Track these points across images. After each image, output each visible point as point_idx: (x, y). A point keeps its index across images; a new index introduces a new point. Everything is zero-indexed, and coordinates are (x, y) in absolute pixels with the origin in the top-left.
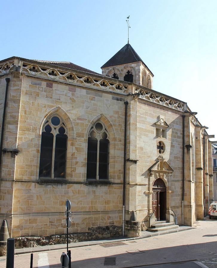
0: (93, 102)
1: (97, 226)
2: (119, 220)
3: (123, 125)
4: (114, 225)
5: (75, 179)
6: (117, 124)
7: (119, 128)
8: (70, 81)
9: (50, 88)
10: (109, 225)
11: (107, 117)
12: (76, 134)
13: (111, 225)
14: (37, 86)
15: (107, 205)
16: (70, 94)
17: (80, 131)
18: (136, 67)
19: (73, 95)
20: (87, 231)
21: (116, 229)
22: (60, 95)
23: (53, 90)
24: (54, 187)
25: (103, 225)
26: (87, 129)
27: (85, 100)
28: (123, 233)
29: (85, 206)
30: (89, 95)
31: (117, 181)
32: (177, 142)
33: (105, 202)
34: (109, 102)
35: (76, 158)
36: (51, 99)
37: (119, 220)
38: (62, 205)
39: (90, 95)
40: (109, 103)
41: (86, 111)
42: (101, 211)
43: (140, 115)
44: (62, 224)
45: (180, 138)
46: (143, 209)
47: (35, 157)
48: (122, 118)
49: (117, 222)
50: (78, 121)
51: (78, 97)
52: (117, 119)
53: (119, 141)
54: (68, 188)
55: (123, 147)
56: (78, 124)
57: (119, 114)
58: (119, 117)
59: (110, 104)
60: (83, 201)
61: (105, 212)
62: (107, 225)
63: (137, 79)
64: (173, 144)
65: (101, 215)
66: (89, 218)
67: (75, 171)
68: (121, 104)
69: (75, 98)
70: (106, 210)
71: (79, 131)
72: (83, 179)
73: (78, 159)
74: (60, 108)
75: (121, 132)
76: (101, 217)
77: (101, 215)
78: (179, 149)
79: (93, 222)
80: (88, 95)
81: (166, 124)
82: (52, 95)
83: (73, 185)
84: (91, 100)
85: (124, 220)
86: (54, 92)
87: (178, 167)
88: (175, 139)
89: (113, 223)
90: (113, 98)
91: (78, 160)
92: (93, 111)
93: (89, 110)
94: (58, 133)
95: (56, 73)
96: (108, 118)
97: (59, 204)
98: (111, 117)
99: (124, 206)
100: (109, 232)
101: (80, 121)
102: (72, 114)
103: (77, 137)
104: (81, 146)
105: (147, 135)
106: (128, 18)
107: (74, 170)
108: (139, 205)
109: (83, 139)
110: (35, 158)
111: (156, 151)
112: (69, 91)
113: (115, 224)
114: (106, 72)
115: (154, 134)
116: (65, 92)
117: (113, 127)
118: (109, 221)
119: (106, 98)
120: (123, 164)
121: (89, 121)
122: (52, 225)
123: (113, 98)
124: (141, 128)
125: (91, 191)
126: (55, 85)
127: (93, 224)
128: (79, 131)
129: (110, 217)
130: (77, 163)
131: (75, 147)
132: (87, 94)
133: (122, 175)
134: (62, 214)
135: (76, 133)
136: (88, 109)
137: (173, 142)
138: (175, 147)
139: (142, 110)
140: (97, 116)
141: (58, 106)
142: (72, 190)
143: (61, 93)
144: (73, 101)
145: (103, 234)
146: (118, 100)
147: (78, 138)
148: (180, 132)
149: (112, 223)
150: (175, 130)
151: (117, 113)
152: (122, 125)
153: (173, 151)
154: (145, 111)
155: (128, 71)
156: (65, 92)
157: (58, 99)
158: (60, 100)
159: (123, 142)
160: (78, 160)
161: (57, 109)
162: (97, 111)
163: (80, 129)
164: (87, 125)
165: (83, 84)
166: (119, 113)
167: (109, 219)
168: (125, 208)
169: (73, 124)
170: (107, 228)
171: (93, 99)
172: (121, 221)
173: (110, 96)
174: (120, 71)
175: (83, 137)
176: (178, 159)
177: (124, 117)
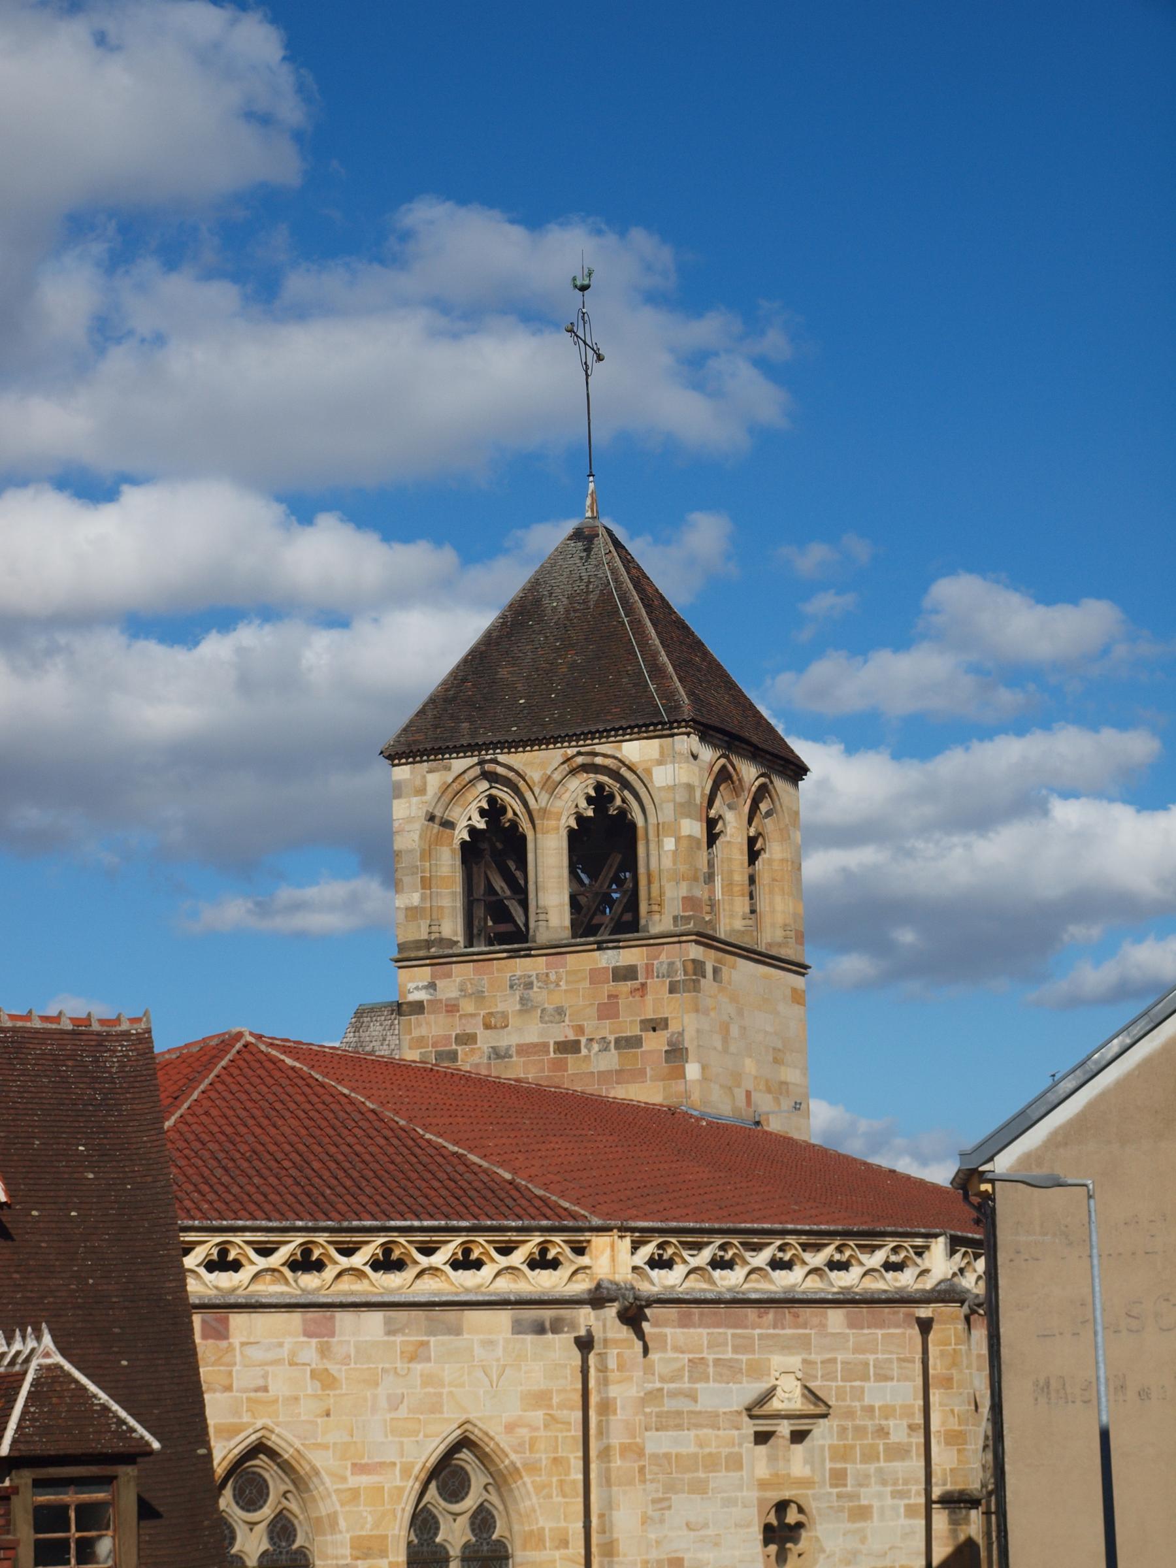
3: (572, 1461)
6: (544, 1458)
7: (554, 1480)
8: (310, 1281)
9: (218, 1342)
11: (492, 1434)
12: (351, 1548)
16: (309, 1352)
17: (368, 1526)
18: (660, 762)
19: (324, 1351)
22: (266, 1364)
23: (234, 1349)
26: (399, 1515)
27: (381, 1366)
30: (399, 1339)
32: (884, 1483)
34: (500, 1352)
36: (226, 1394)
39: (404, 1334)
40: (498, 1360)
41: (392, 1419)
43: (658, 1385)
45: (908, 1452)
48: (569, 1423)
50: (354, 1481)
52: (542, 1433)
53: (557, 1548)
56: (355, 1493)
57: (550, 1407)
58: (550, 1421)
59: (502, 1363)
63: (667, 863)
64: (864, 1502)
68: (561, 1346)
69: (333, 1368)
71: (362, 1528)
74: (272, 1432)
75: (564, 1496)
78: (903, 1521)
80: (392, 1338)
81: (812, 1398)
82: (230, 1373)
86: (238, 1358)
88: (872, 1468)
90: (518, 1328)
92: (421, 1417)
93: (403, 1412)
94: (265, 1545)
95: (240, 1258)
96: (497, 1438)
98: (510, 1428)
101: (364, 1480)
102: (325, 1447)
103: (357, 1558)
105: (699, 1488)
106: (584, 288)
112: (305, 1339)
114: (422, 791)
116: (287, 1347)
117: (527, 1479)
119: (481, 1337)
121: (406, 1472)
123: (518, 1328)
124: (667, 1456)
126: (237, 1320)
128: (362, 1528)
132: (389, 1333)
135: (351, 1538)
136: (397, 1409)
137: (863, 1490)
139: (671, 1354)
140: (445, 1435)
141: (259, 1425)
143: (270, 1356)
144: (325, 1380)
146: (540, 1329)
147: (359, 1562)
148: (905, 1423)
150: (872, 1418)
151: (541, 1399)
152: (568, 1459)
153: (863, 1540)
154: (687, 1356)
155: (599, 787)
156: (288, 1342)
157: (257, 1390)
158: (265, 1389)
161: (259, 1435)
162: (442, 1413)
163: (369, 1519)
164: (401, 1489)
165: (366, 1282)
166: (551, 1399)
169: (334, 1497)
171: (417, 1354)
173: (504, 1317)
174: (537, 790)
175: (383, 1554)
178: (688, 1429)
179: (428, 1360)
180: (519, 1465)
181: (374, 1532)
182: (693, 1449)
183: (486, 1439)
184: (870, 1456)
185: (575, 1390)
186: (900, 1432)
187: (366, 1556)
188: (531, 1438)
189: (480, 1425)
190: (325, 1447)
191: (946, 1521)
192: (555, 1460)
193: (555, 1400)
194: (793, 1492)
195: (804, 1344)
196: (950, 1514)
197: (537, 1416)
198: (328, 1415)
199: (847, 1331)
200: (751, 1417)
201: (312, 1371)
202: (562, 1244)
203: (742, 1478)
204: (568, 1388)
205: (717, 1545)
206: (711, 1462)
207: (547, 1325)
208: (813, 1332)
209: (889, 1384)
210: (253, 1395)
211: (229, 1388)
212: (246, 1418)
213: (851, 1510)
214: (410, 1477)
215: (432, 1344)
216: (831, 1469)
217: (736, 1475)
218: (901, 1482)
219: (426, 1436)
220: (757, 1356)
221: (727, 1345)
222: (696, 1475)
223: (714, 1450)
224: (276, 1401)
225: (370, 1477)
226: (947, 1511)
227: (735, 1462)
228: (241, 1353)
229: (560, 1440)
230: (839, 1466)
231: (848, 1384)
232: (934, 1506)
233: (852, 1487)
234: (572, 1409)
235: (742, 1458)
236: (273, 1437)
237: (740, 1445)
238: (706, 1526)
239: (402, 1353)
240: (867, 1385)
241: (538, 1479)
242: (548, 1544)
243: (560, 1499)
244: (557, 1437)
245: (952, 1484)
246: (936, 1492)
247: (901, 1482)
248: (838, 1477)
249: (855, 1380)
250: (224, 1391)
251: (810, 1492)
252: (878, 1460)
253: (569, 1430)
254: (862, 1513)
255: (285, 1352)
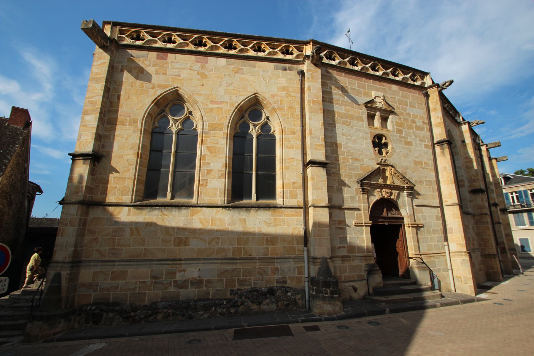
0: (239, 75)
1: (249, 287)
2: (296, 275)
3: (297, 108)
4: (286, 285)
5: (205, 199)
10: (275, 284)
11: (266, 97)
13: (279, 285)
14: (141, 59)
15: (270, 247)
16: (197, 67)
17: (216, 121)
19: (202, 67)
20: (229, 296)
21: (289, 294)
24: (164, 214)
25: (264, 287)
28: (307, 302)
29: (226, 247)
30: (232, 66)
31: (289, 202)
33: (267, 241)
35: (209, 164)
37: (296, 275)
38: (178, 246)
39: (233, 65)
42: (259, 259)
44: (175, 282)
46: (351, 255)
47: (132, 165)
48: (296, 97)
49: (292, 279)
50: (211, 106)
51: (211, 70)
53: (291, 134)
54: (192, 215)
55: (300, 143)
56: (212, 110)
57: (288, 91)
60: (220, 237)
61: (267, 259)
62: (272, 286)
65: (257, 265)
66: (233, 270)
67: (206, 185)
69: (206, 73)
70: (270, 256)
71: (213, 121)
72: (220, 199)
73: (212, 165)
76: (259, 268)
77: (257, 264)
79: (242, 278)
82: (166, 70)
83: (202, 210)
84: (236, 73)
85: (306, 275)
86: (170, 66)
87: (426, 181)
89: (285, 282)
91: (212, 166)
92: (239, 90)
93: (231, 87)
97: (172, 242)
98: (273, 96)
99: (306, 249)
100: (273, 300)
101: (215, 106)
103: (211, 130)
104: (218, 143)
107: (205, 184)
108: (340, 247)
109: (221, 133)
110: (132, 167)
111: (371, 150)
112: (196, 63)
113: (289, 284)
115: (363, 121)
116: (189, 64)
118: (276, 277)
120: (301, 171)
122: (155, 282)
125: (237, 220)
127: (241, 283)
129: (277, 269)
130: (209, 172)
131: (207, 147)
133: (300, 192)
134: (178, 262)
138: (412, 145)
140: (248, 96)
141: (175, 86)
142: (200, 219)
143: (182, 66)
145: (260, 304)
147: (211, 132)
149: (281, 280)
151: (285, 89)
159: (299, 134)
160: (212, 166)
163: (216, 118)
166: (288, 89)
167: (275, 274)
168: (308, 251)
170: (271, 291)
172: (302, 277)
175: (221, 129)
176: (424, 166)
177: (299, 95)
178: (342, 105)
179: (243, 74)
180: (276, 107)
181: (218, 122)
182: (344, 112)
183: (264, 99)
184: (410, 128)
185: (298, 87)
186: (419, 123)
187: (215, 129)
188: (281, 100)
189: (261, 94)
190: (201, 95)
191: (440, 149)
192: (290, 107)
193: (290, 90)
194: (383, 132)
195: (384, 91)
196: (440, 147)
197: (284, 94)
198: (203, 85)
199: (399, 91)
200: (366, 107)
201: (197, 72)
202: (293, 47)
203: (363, 124)
204: (295, 87)
205: (354, 142)
206: (352, 117)
207: (287, 68)
208: (387, 88)
209: (415, 109)
210: (174, 77)
211: (165, 74)
212: (171, 83)
213: (405, 141)
214: (233, 107)
215: (244, 69)
216: (396, 128)
217: (362, 123)
218: (422, 137)
219: (240, 95)
220: (367, 91)
221: (355, 85)
222: (345, 119)
223: (352, 114)
224: (183, 79)
225: (217, 105)
226: (439, 146)
227: (360, 119)
228: (171, 65)
229: (292, 101)
230: (399, 128)
231: (401, 106)
232: (435, 145)
233: (405, 135)
234: (297, 93)
235: (363, 118)
236: (181, 90)
237: (362, 114)
238: (350, 135)
239: (232, 70)
240: (407, 107)
241: (283, 112)
242: (287, 133)
243: (292, 119)
244: (291, 101)
245: (440, 138)
246: (435, 141)
247: (422, 137)
248: (399, 131)
249: (403, 105)
250: (163, 75)
251: (389, 133)
252: (413, 129)
253: (296, 99)
254: (409, 143)
255: (188, 66)
